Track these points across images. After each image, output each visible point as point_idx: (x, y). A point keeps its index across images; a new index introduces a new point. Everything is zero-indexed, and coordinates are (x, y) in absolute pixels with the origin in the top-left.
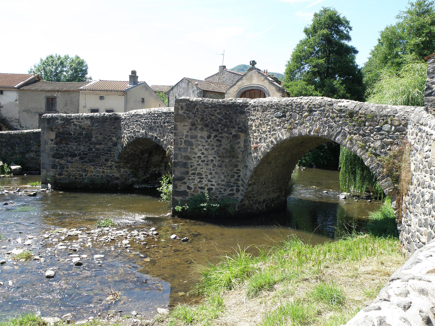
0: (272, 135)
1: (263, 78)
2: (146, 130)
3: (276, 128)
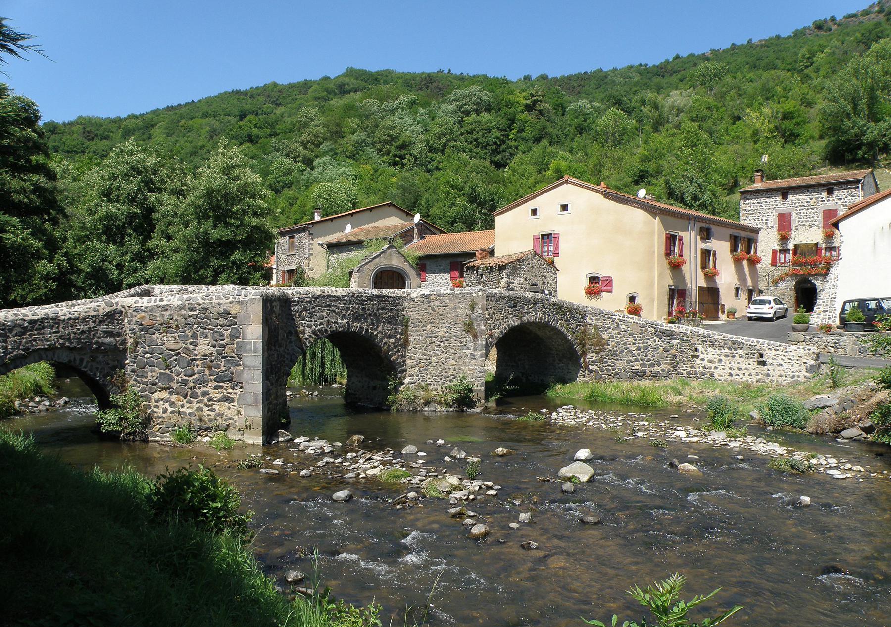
1: (403, 260)
3: (509, 316)
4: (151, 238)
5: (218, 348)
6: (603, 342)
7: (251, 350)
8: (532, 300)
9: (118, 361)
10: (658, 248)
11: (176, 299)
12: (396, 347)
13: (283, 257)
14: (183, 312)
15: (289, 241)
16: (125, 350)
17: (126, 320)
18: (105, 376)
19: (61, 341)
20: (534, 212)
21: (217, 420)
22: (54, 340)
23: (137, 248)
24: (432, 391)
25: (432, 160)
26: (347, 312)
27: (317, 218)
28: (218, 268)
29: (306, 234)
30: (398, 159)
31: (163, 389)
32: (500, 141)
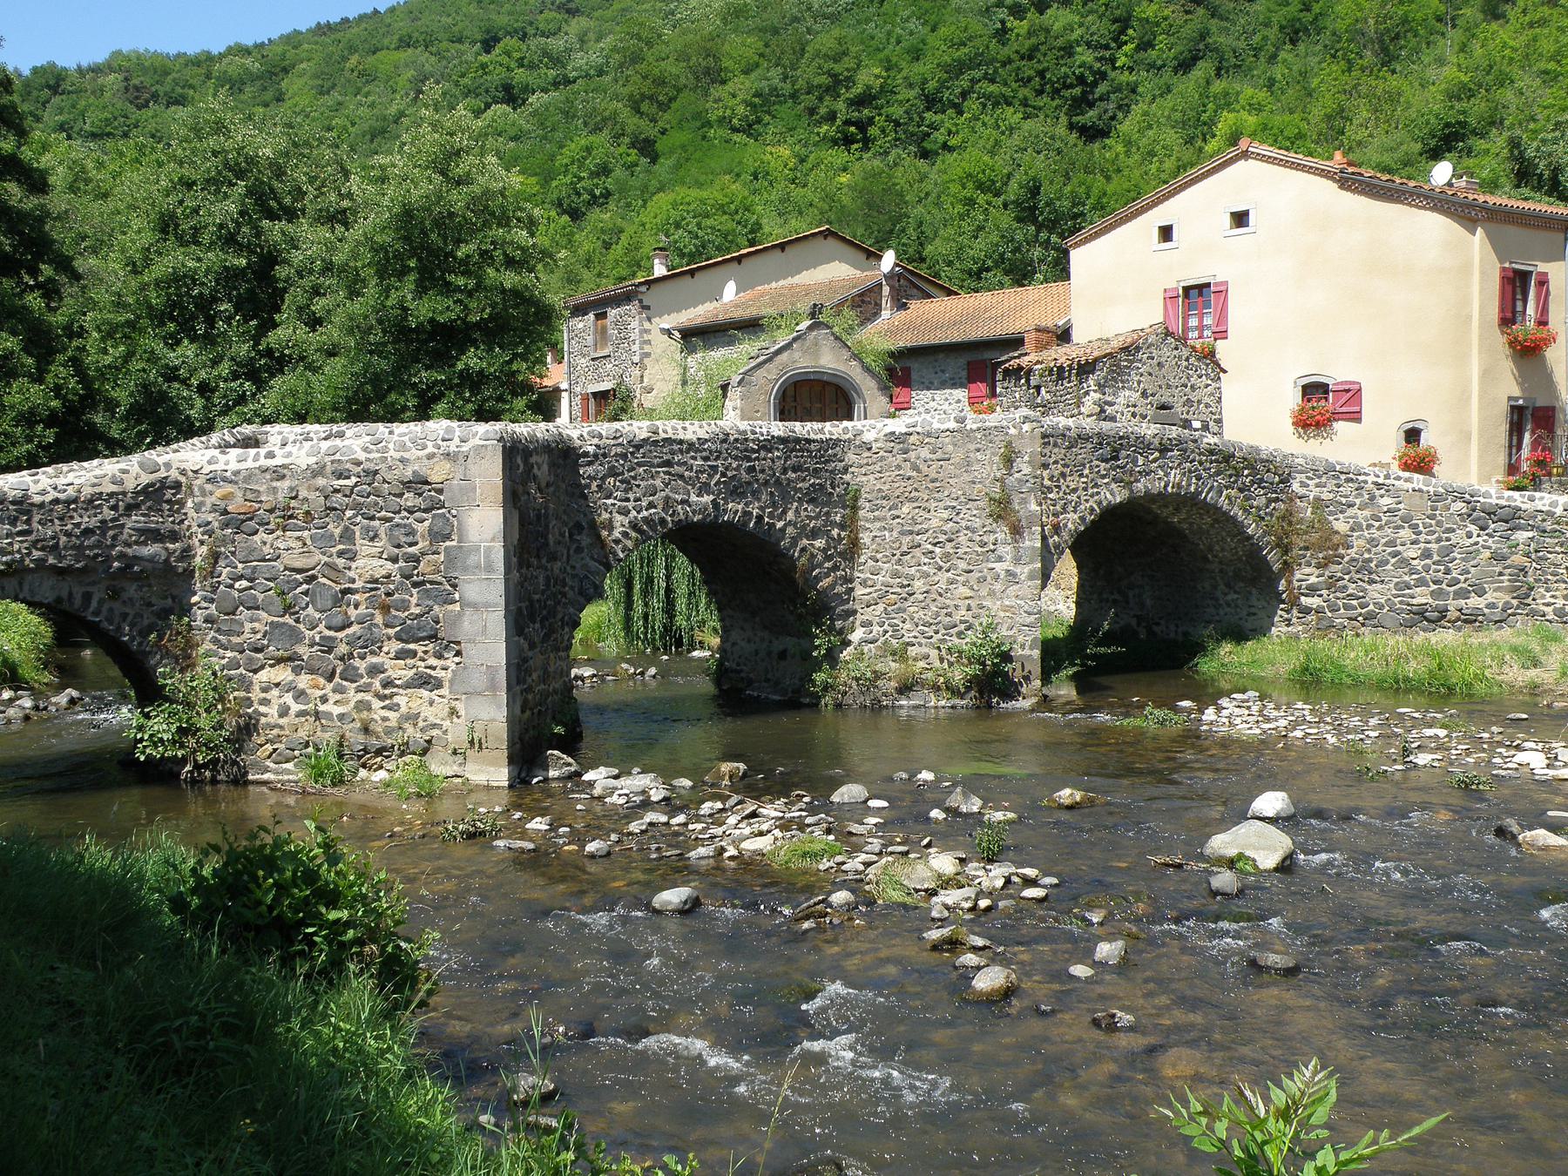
0: (1092, 496)
1: (846, 354)
2: (718, 495)
3: (1100, 481)
4: (275, 326)
5: (402, 564)
6: (1336, 539)
7: (478, 567)
8: (1156, 441)
9: (174, 598)
10: (1482, 308)
11: (303, 452)
12: (828, 558)
13: (583, 362)
14: (321, 482)
15: (596, 325)
16: (189, 573)
17: (190, 504)
18: (144, 634)
19: (36, 554)
20: (1166, 233)
21: (404, 731)
22: (19, 551)
23: (243, 349)
24: (915, 660)
25: (934, 127)
26: (711, 476)
27: (660, 270)
28: (429, 388)
29: (632, 308)
30: (852, 129)
31: (280, 661)
32: (1094, 73)
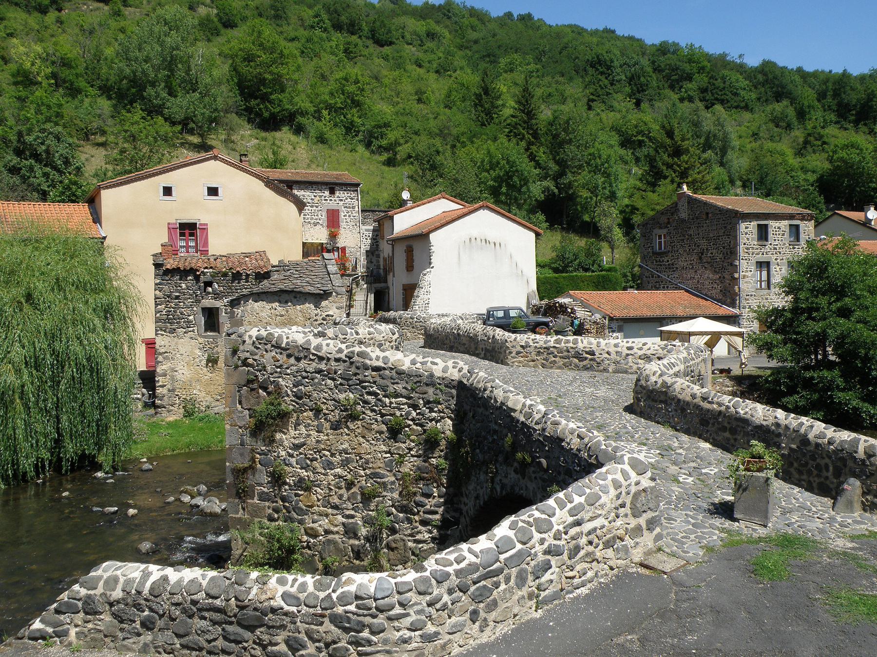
20: (168, 191)
